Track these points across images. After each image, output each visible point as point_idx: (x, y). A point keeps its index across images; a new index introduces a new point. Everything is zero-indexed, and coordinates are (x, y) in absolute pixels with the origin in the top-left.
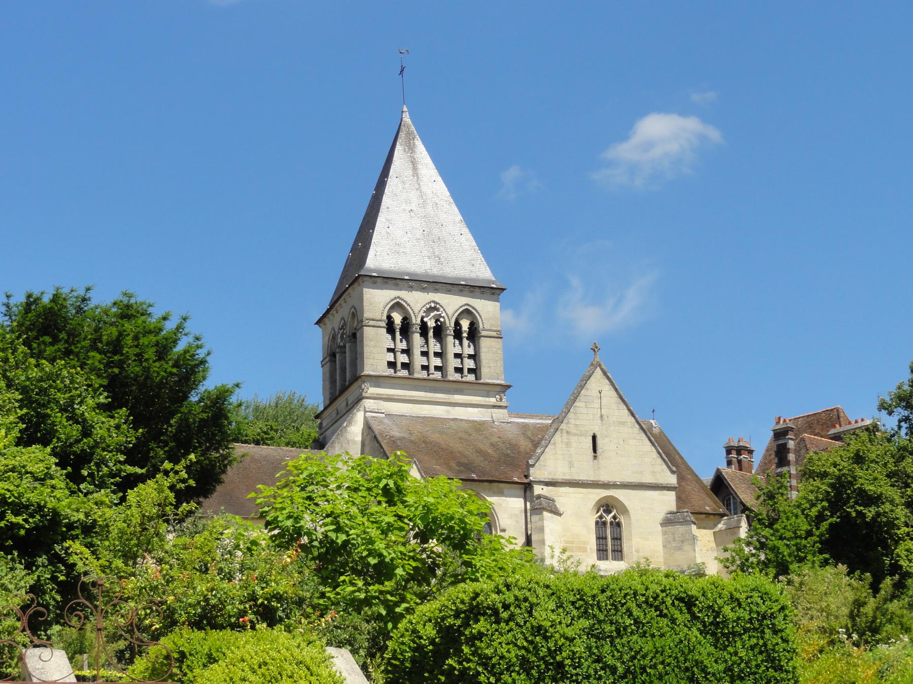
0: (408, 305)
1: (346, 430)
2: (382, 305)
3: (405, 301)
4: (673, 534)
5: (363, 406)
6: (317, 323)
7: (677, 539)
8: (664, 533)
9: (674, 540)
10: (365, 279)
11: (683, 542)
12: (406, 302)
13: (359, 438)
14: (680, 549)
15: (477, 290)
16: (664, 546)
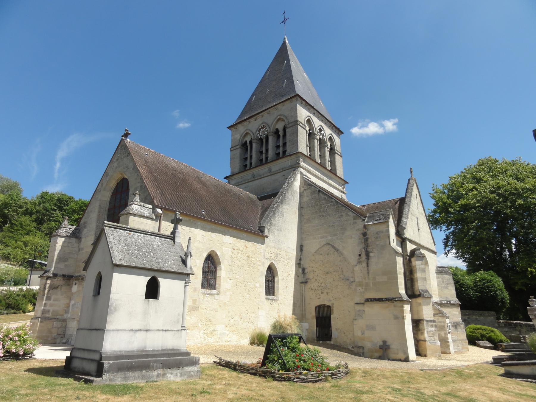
0: (313, 122)
1: (293, 183)
2: (304, 117)
3: (312, 120)
4: (442, 279)
5: (299, 171)
6: (228, 128)
7: (445, 282)
8: (438, 278)
9: (443, 282)
10: (299, 99)
11: (448, 284)
12: (313, 121)
13: (298, 191)
14: (447, 288)
15: (334, 128)
16: (438, 285)
